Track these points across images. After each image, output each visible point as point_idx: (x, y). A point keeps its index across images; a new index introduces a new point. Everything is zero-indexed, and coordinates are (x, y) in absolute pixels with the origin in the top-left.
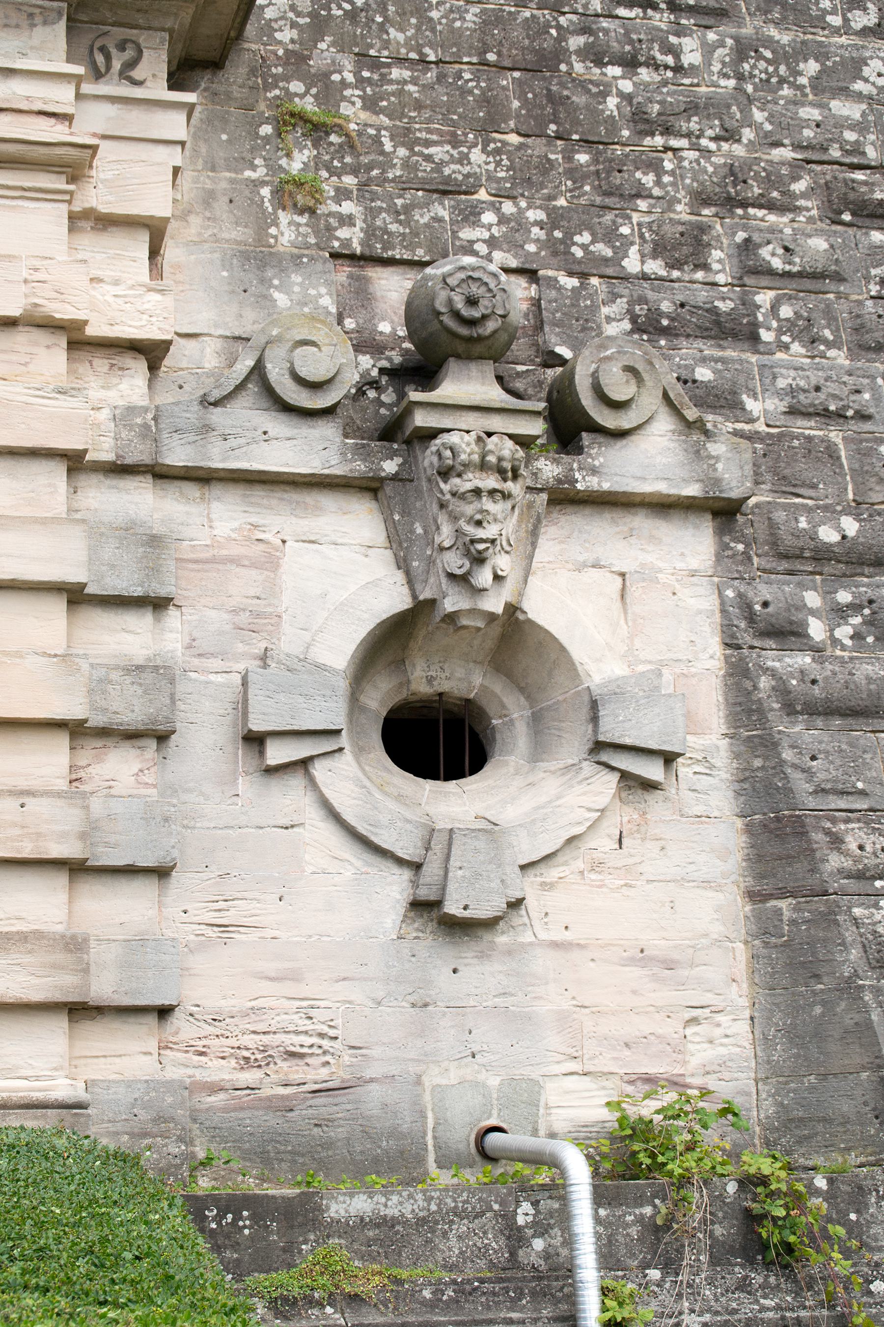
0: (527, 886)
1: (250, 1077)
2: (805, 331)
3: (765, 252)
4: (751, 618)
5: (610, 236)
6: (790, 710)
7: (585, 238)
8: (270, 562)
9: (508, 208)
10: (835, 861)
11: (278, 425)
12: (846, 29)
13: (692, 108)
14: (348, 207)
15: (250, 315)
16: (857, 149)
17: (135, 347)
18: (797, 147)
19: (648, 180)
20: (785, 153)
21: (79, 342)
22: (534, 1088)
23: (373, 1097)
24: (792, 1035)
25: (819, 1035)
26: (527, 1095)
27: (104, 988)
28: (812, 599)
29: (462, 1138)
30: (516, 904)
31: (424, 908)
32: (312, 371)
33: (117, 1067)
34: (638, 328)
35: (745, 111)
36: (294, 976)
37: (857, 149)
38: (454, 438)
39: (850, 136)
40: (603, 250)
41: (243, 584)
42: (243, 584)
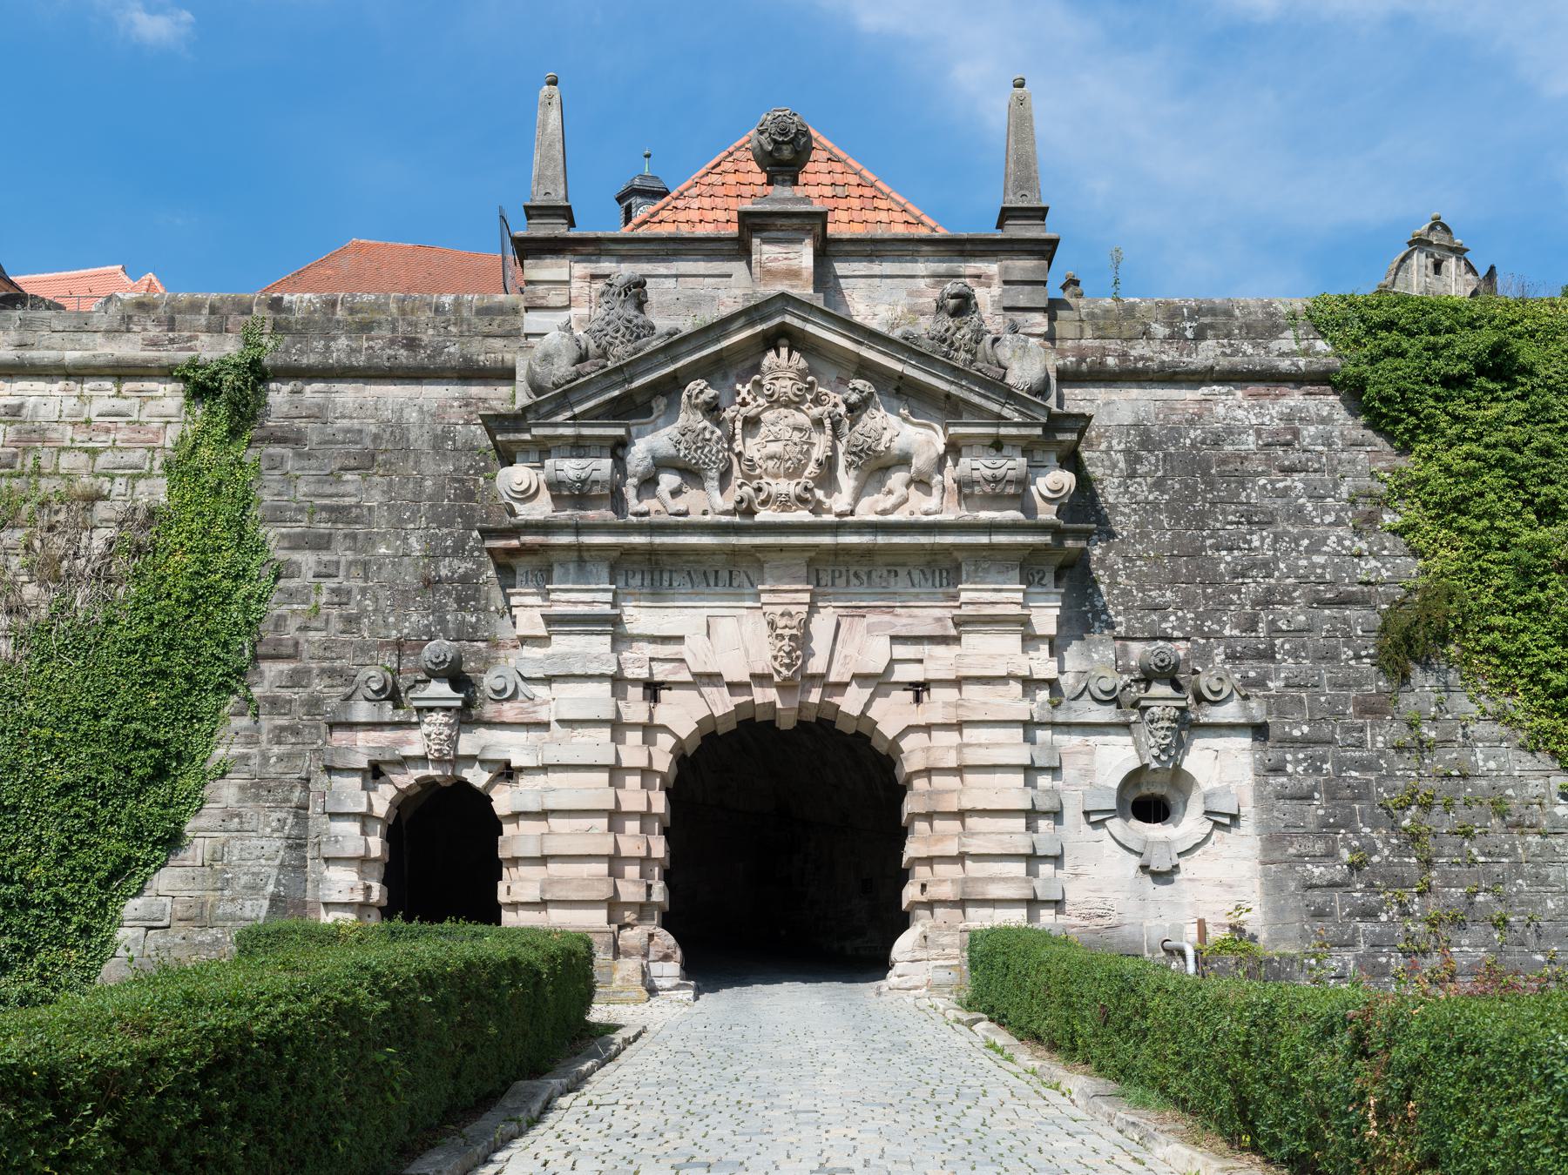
0: (1182, 862)
1: (1085, 923)
2: (1294, 654)
5: (1219, 622)
8: (1092, 753)
9: (1180, 613)
11: (1095, 706)
13: (1254, 566)
16: (1322, 576)
19: (1235, 597)
22: (1182, 927)
23: (1126, 930)
25: (1283, 910)
28: (1289, 757)
29: (1156, 943)
31: (1144, 868)
32: (1108, 687)
35: (1276, 564)
36: (1100, 890)
37: (1322, 576)
40: (1216, 627)
41: (1082, 760)
42: (1082, 760)
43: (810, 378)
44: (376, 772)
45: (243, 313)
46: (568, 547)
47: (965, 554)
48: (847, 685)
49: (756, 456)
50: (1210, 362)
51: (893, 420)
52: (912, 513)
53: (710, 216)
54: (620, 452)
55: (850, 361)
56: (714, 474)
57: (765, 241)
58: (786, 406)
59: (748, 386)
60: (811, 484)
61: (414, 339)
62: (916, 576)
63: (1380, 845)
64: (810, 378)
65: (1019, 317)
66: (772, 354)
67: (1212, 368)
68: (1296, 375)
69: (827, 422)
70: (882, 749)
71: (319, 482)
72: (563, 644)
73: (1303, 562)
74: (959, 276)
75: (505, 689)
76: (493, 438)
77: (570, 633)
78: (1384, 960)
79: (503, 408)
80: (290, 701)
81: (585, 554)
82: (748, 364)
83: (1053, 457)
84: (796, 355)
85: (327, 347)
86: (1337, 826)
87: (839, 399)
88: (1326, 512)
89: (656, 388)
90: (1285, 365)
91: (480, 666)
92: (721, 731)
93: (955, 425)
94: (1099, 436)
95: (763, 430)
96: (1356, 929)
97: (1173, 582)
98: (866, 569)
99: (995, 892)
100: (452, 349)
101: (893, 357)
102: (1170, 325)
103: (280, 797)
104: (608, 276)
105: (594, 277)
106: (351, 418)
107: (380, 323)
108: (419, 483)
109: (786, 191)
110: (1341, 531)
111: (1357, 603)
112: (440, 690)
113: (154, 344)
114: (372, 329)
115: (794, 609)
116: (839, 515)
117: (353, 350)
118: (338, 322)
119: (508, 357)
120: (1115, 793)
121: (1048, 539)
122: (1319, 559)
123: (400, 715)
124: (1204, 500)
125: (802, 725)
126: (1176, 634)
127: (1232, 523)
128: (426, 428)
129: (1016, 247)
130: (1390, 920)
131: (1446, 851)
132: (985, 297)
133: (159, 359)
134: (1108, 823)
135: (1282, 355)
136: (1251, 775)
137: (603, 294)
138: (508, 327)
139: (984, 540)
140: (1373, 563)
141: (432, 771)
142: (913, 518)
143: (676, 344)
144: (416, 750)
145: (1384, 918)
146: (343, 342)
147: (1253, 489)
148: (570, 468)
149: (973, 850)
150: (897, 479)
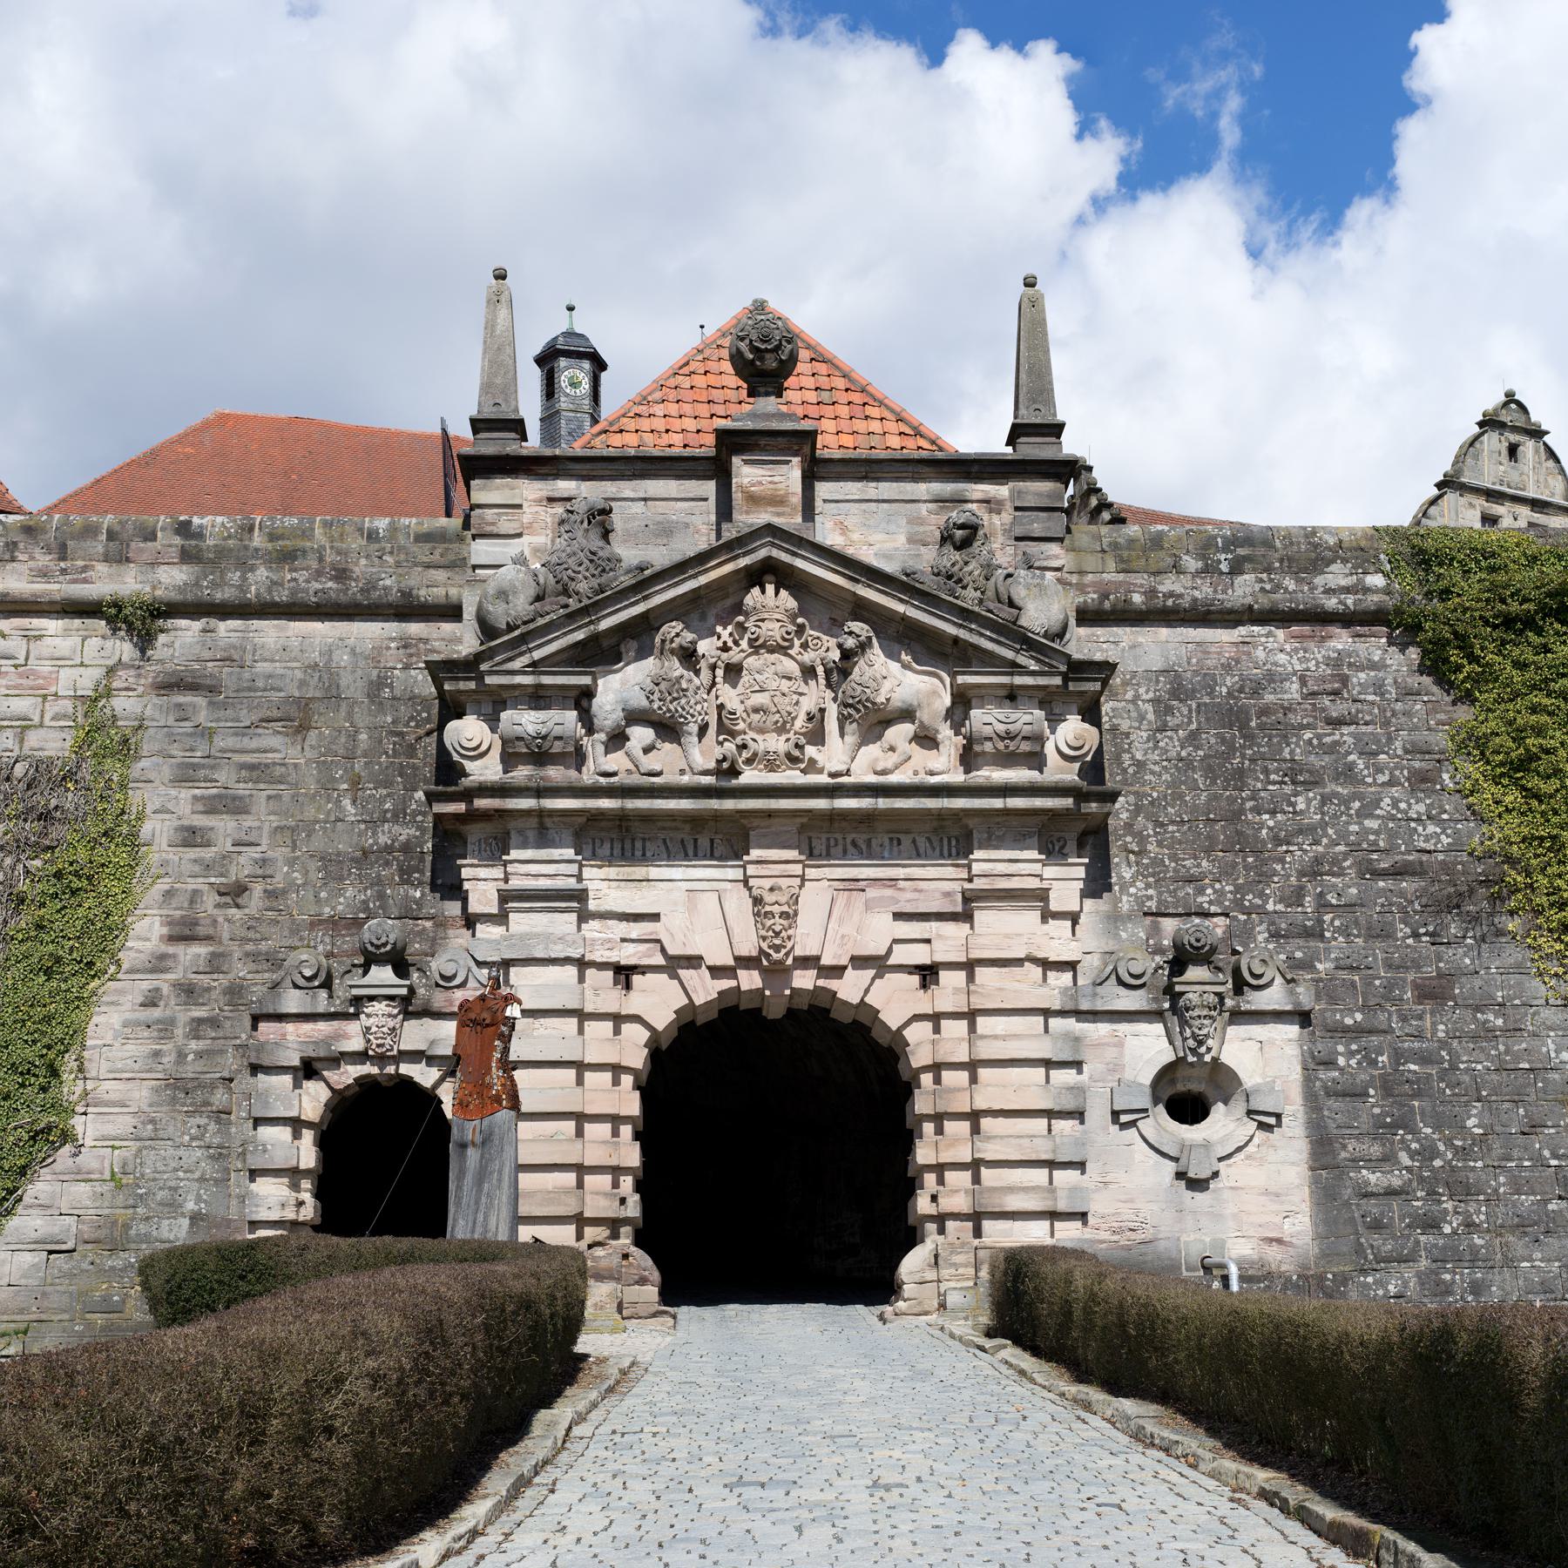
1: (1116, 1238)
2: (1345, 931)
3: (1329, 897)
4: (1313, 1057)
5: (1261, 895)
6: (1328, 1095)
7: (1250, 897)
8: (1120, 1045)
9: (1217, 886)
10: (1343, 1155)
11: (1122, 991)
12: (1375, 783)
13: (1300, 832)
14: (1151, 892)
15: (1111, 942)
16: (1375, 843)
17: (1067, 963)
18: (1347, 845)
19: (1278, 867)
20: (1341, 848)
21: (1046, 965)
23: (1162, 1245)
24: (1326, 1222)
26: (1220, 1245)
27: (1062, 1206)
28: (1341, 1048)
30: (1216, 1174)
31: (1180, 1175)
32: (1136, 970)
33: (1069, 1233)
34: (1272, 936)
36: (1132, 1201)
37: (1375, 843)
38: (1190, 996)
39: (1372, 837)
40: (1258, 901)
41: (1111, 1053)
42: (1111, 1053)
43: (800, 620)
44: (308, 1070)
45: (146, 540)
46: (527, 813)
47: (976, 820)
48: (845, 967)
49: (740, 709)
50: (1249, 600)
51: (894, 666)
52: (916, 773)
53: (677, 424)
54: (584, 703)
55: (844, 600)
56: (694, 728)
57: (746, 462)
58: (771, 651)
59: (730, 628)
60: (803, 741)
61: (344, 570)
62: (922, 842)
63: (1442, 1148)
64: (800, 620)
65: (1032, 548)
66: (756, 591)
67: (1251, 607)
68: (1343, 614)
69: (820, 670)
70: (884, 1041)
71: (236, 734)
72: (521, 922)
73: (1354, 828)
74: (966, 501)
75: (454, 976)
76: (439, 687)
77: (530, 910)
78: (1448, 1277)
79: (442, 652)
80: (208, 989)
81: (548, 822)
82: (729, 602)
83: (1074, 708)
84: (783, 593)
85: (244, 579)
86: (1395, 1126)
87: (833, 642)
88: (1379, 770)
89: (626, 631)
90: (1331, 603)
91: (425, 947)
92: (701, 1020)
93: (964, 673)
94: (1125, 683)
95: (745, 678)
96: (1417, 1242)
97: (1208, 851)
98: (865, 836)
99: (1015, 1203)
100: (388, 582)
101: (894, 597)
102: (1203, 557)
103: (199, 1100)
104: (569, 499)
105: (551, 500)
106: (273, 661)
107: (304, 552)
108: (353, 737)
109: (769, 404)
110: (1395, 791)
111: (1414, 874)
112: (383, 975)
113: (44, 574)
114: (296, 558)
115: (784, 882)
116: (832, 775)
117: (274, 583)
118: (257, 550)
119: (453, 592)
120: (1148, 1091)
121: (1068, 802)
122: (1372, 824)
124: (1243, 756)
125: (791, 1013)
126: (1213, 909)
127: (1274, 783)
128: (360, 672)
129: (1029, 468)
130: (1454, 1232)
131: (1515, 1154)
132: (996, 524)
133: (50, 592)
134: (1139, 1124)
135: (1329, 591)
136: (1299, 1069)
137: (562, 522)
138: (451, 557)
139: (997, 803)
140: (1431, 829)
141: (369, 1069)
142: (916, 780)
143: (646, 582)
144: (355, 1044)
145: (1447, 1230)
146: (262, 573)
147: (1298, 745)
148: (526, 721)
149: (988, 1156)
150: (900, 733)
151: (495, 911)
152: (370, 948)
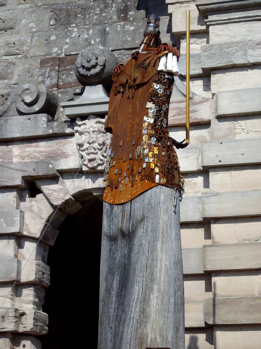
44: (31, 187)
123: (55, 128)
144: (71, 163)
151: (196, 27)
152: (83, 71)
